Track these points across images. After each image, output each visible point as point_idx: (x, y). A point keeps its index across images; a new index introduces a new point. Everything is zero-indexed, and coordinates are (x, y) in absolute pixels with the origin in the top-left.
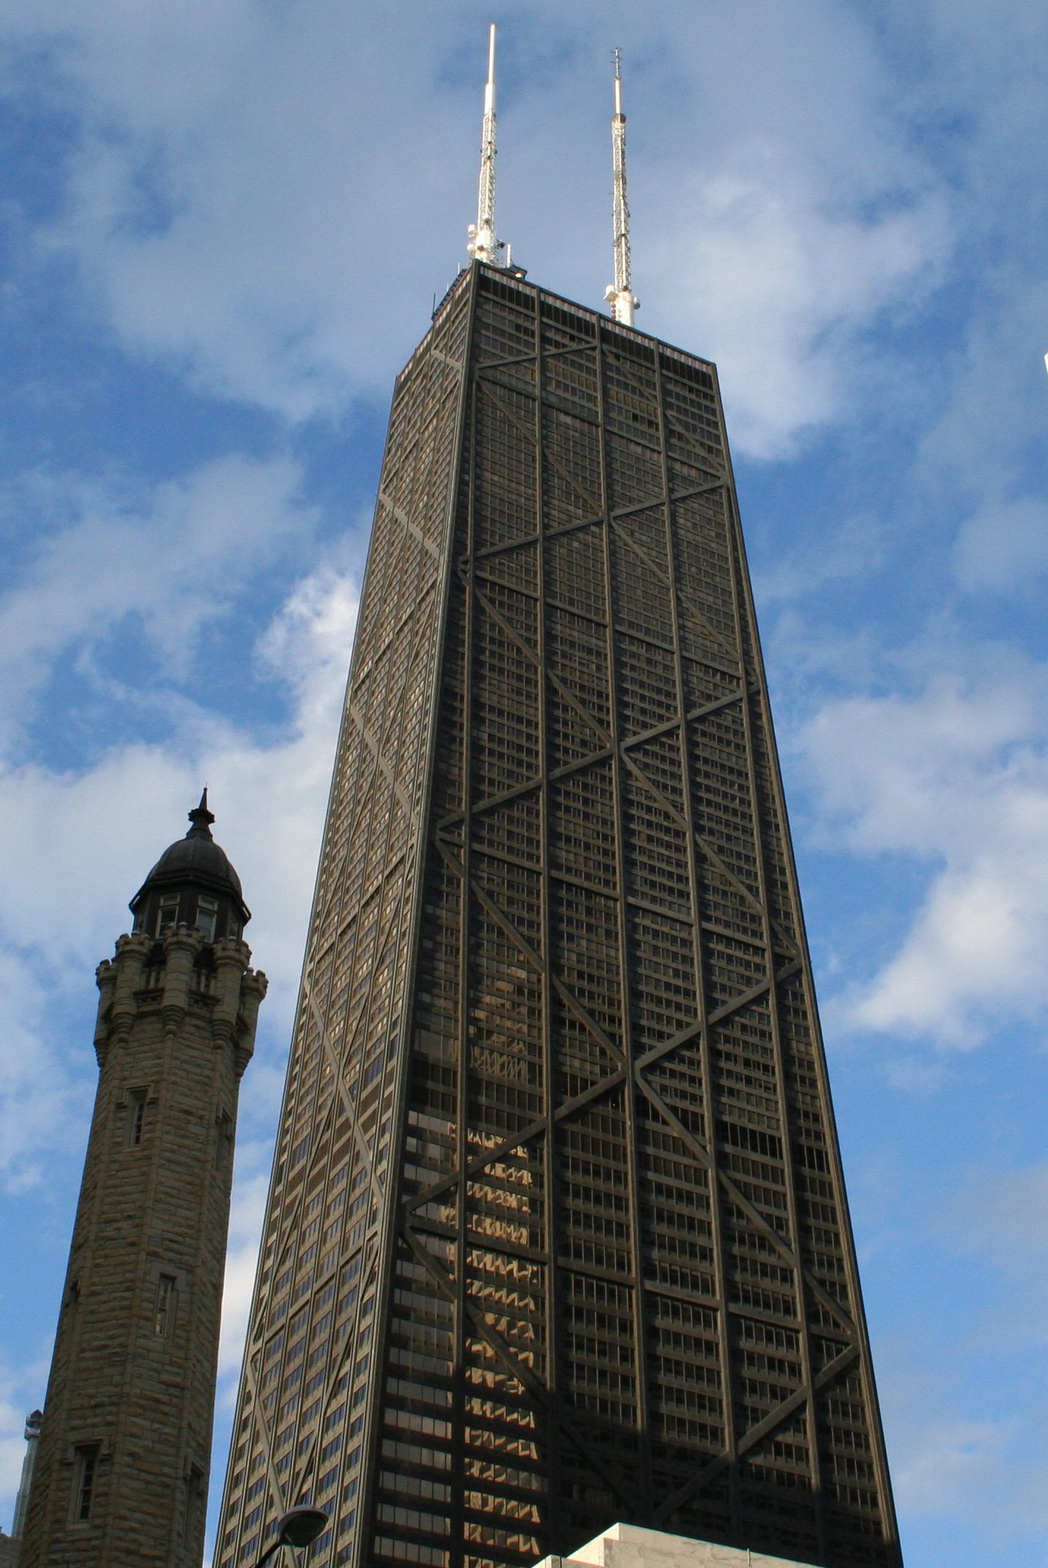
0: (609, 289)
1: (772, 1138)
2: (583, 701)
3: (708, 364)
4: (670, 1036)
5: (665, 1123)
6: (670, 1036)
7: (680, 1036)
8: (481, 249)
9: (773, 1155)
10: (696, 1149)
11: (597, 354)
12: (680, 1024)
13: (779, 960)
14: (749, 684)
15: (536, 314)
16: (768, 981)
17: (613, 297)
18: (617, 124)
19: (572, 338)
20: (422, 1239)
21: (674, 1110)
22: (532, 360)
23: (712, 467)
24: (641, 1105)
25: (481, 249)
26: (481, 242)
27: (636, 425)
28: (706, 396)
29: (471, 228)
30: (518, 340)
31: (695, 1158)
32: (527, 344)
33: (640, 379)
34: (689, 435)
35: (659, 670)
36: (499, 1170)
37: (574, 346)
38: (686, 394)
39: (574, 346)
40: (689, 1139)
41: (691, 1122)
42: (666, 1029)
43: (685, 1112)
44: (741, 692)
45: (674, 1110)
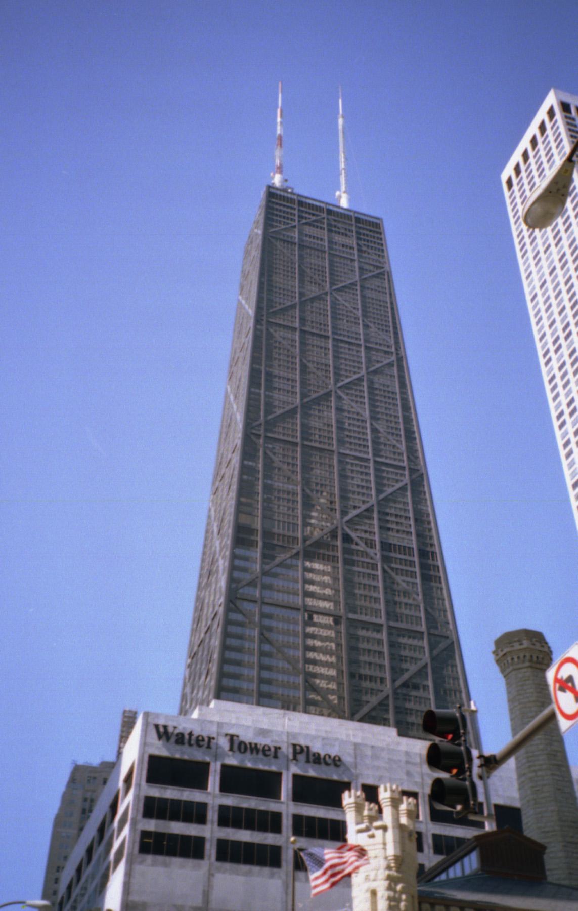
1: (409, 548)
2: (318, 369)
5: (357, 544)
7: (364, 507)
9: (410, 555)
10: (372, 555)
11: (325, 221)
12: (364, 502)
13: (412, 471)
14: (397, 354)
15: (296, 206)
16: (406, 480)
19: (313, 215)
24: (347, 539)
27: (344, 249)
28: (378, 233)
31: (372, 558)
32: (292, 219)
34: (370, 250)
35: (355, 353)
37: (314, 218)
38: (368, 233)
39: (314, 218)
40: (369, 550)
41: (370, 544)
43: (366, 539)
44: (394, 358)
45: (361, 538)
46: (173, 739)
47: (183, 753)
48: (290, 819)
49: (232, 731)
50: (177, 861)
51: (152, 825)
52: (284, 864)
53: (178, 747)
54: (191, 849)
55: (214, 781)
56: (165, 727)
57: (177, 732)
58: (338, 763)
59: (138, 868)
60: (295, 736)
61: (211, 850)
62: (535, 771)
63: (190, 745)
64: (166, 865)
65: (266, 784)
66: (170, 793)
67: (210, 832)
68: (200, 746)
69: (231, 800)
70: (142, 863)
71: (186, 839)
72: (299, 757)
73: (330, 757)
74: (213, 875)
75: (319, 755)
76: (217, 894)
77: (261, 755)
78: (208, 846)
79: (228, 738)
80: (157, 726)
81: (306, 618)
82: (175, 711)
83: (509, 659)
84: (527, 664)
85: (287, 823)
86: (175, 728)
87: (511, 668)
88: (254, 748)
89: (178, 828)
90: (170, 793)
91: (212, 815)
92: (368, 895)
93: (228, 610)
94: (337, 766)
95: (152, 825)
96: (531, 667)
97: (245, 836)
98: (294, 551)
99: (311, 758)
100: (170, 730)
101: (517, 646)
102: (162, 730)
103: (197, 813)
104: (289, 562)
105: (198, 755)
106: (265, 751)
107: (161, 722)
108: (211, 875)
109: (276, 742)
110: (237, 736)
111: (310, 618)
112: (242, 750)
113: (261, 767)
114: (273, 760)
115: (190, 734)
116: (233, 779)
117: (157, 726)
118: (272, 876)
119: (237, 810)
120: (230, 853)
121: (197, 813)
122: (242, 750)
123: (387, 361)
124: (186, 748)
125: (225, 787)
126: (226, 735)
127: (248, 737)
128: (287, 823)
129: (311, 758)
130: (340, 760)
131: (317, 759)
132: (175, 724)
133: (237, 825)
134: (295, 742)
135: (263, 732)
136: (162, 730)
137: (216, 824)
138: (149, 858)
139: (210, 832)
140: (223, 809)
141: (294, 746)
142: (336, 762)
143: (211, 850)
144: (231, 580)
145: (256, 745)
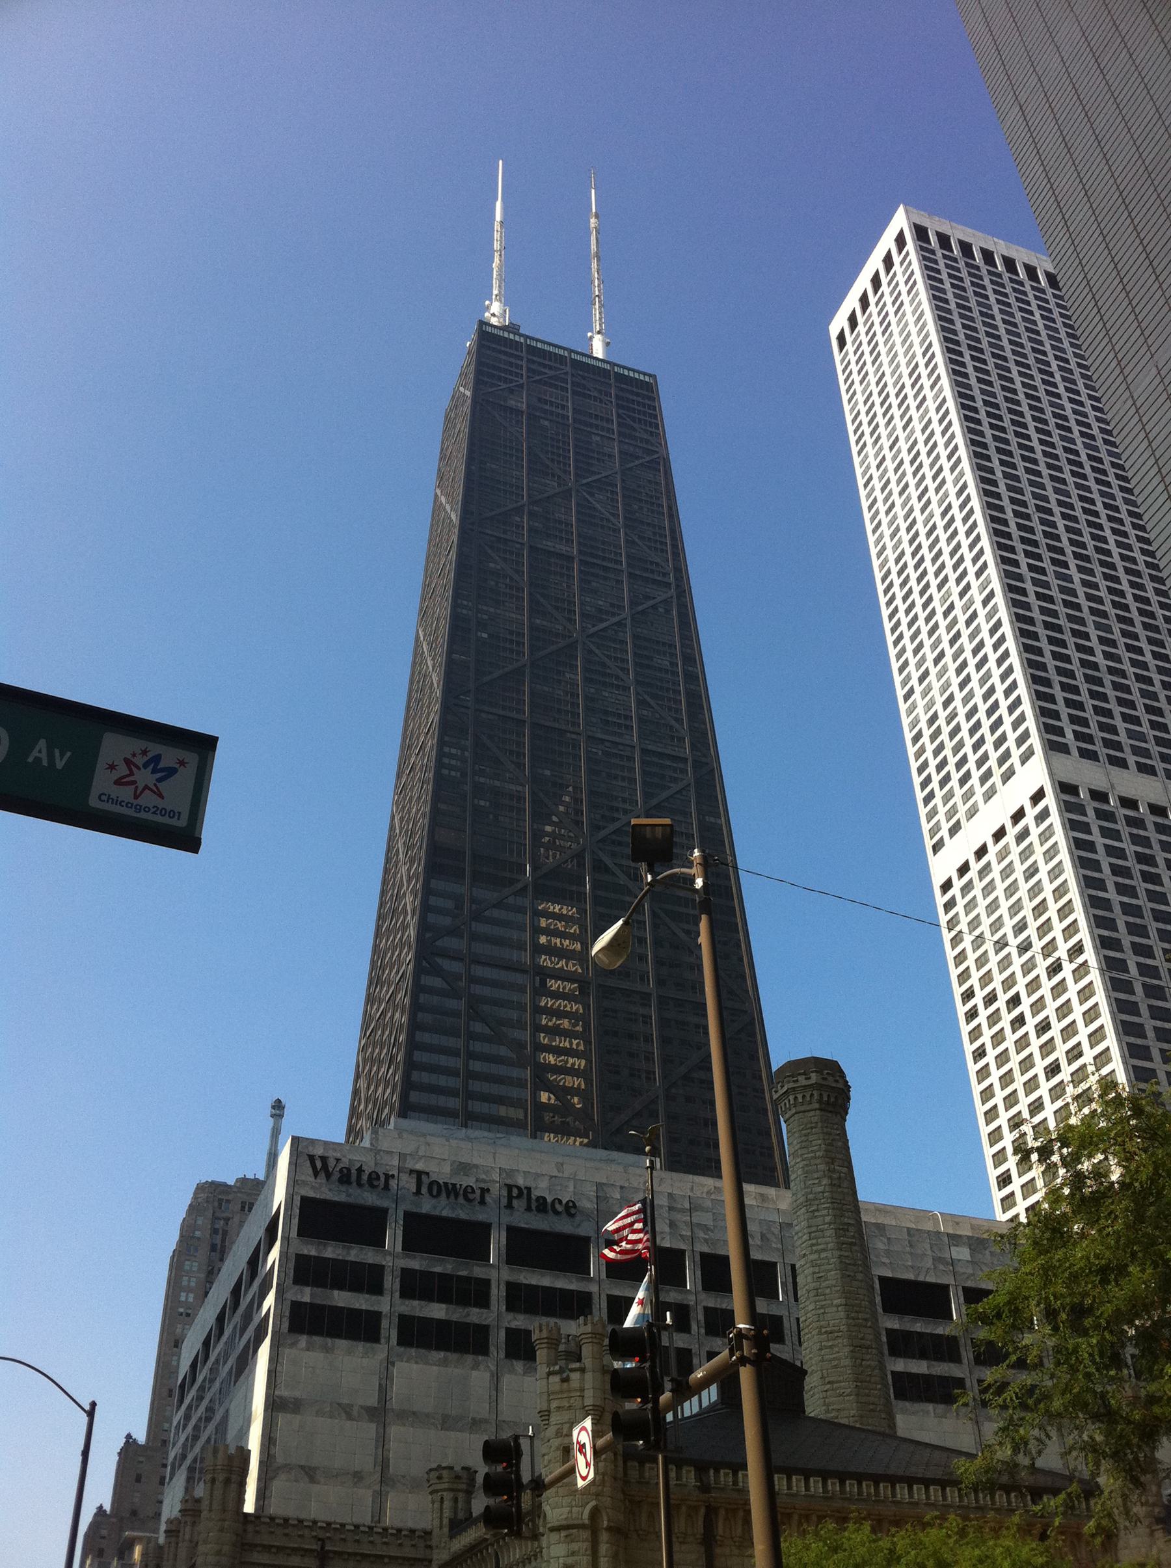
0: (589, 334)
3: (650, 375)
4: (618, 819)
5: (614, 874)
6: (618, 819)
8: (493, 315)
13: (697, 765)
17: (591, 338)
18: (593, 220)
20: (439, 960)
21: (620, 866)
22: (521, 386)
23: (652, 445)
25: (493, 315)
26: (496, 312)
29: (487, 303)
30: (511, 373)
33: (600, 392)
36: (496, 913)
42: (616, 815)
45: (620, 866)
46: (336, 1176)
47: (349, 1195)
48: (503, 1288)
49: (420, 1166)
50: (342, 1343)
51: (306, 1295)
52: (492, 1349)
53: (343, 1188)
54: (363, 1328)
55: (393, 1238)
56: (324, 1159)
57: (341, 1165)
58: (573, 1211)
59: (287, 1352)
60: (511, 1173)
61: (389, 1330)
62: (819, 1252)
63: (360, 1185)
64: (327, 1350)
65: (468, 1239)
66: (332, 1251)
67: (388, 1304)
68: (373, 1186)
69: (416, 1263)
70: (293, 1345)
71: (354, 1314)
72: (515, 1203)
73: (560, 1202)
74: (393, 1364)
75: (544, 1199)
76: (396, 1390)
77: (461, 1200)
78: (384, 1324)
79: (415, 1176)
80: (312, 1158)
81: (537, 985)
82: (339, 1137)
83: (791, 1098)
84: (817, 1106)
85: (497, 1293)
86: (338, 1160)
87: (794, 1111)
88: (451, 1190)
89: (342, 1299)
90: (332, 1251)
91: (391, 1282)
92: (559, 1453)
93: (419, 971)
94: (572, 1216)
95: (306, 1295)
96: (821, 1109)
97: (437, 1311)
98: (519, 886)
99: (534, 1205)
100: (331, 1163)
101: (802, 1081)
102: (319, 1165)
103: (369, 1280)
104: (511, 900)
105: (369, 1198)
106: (468, 1191)
107: (319, 1151)
108: (390, 1363)
109: (484, 1181)
110: (427, 1174)
111: (543, 983)
112: (435, 1193)
113: (463, 1215)
114: (478, 1208)
115: (360, 1170)
116: (423, 1233)
117: (312, 1158)
118: (475, 1367)
119: (426, 1275)
120: (415, 1334)
121: (369, 1280)
122: (435, 1193)
123: (664, 597)
124: (354, 1190)
125: (410, 1245)
126: (412, 1171)
127: (442, 1172)
128: (497, 1293)
129: (534, 1205)
130: (575, 1206)
131: (542, 1206)
132: (338, 1155)
133: (427, 1296)
134: (509, 1182)
135: (463, 1168)
136: (319, 1165)
137: (398, 1294)
138: (303, 1340)
139: (388, 1304)
140: (406, 1273)
141: (510, 1187)
142: (570, 1209)
143: (389, 1330)
144: (424, 927)
145: (454, 1185)
